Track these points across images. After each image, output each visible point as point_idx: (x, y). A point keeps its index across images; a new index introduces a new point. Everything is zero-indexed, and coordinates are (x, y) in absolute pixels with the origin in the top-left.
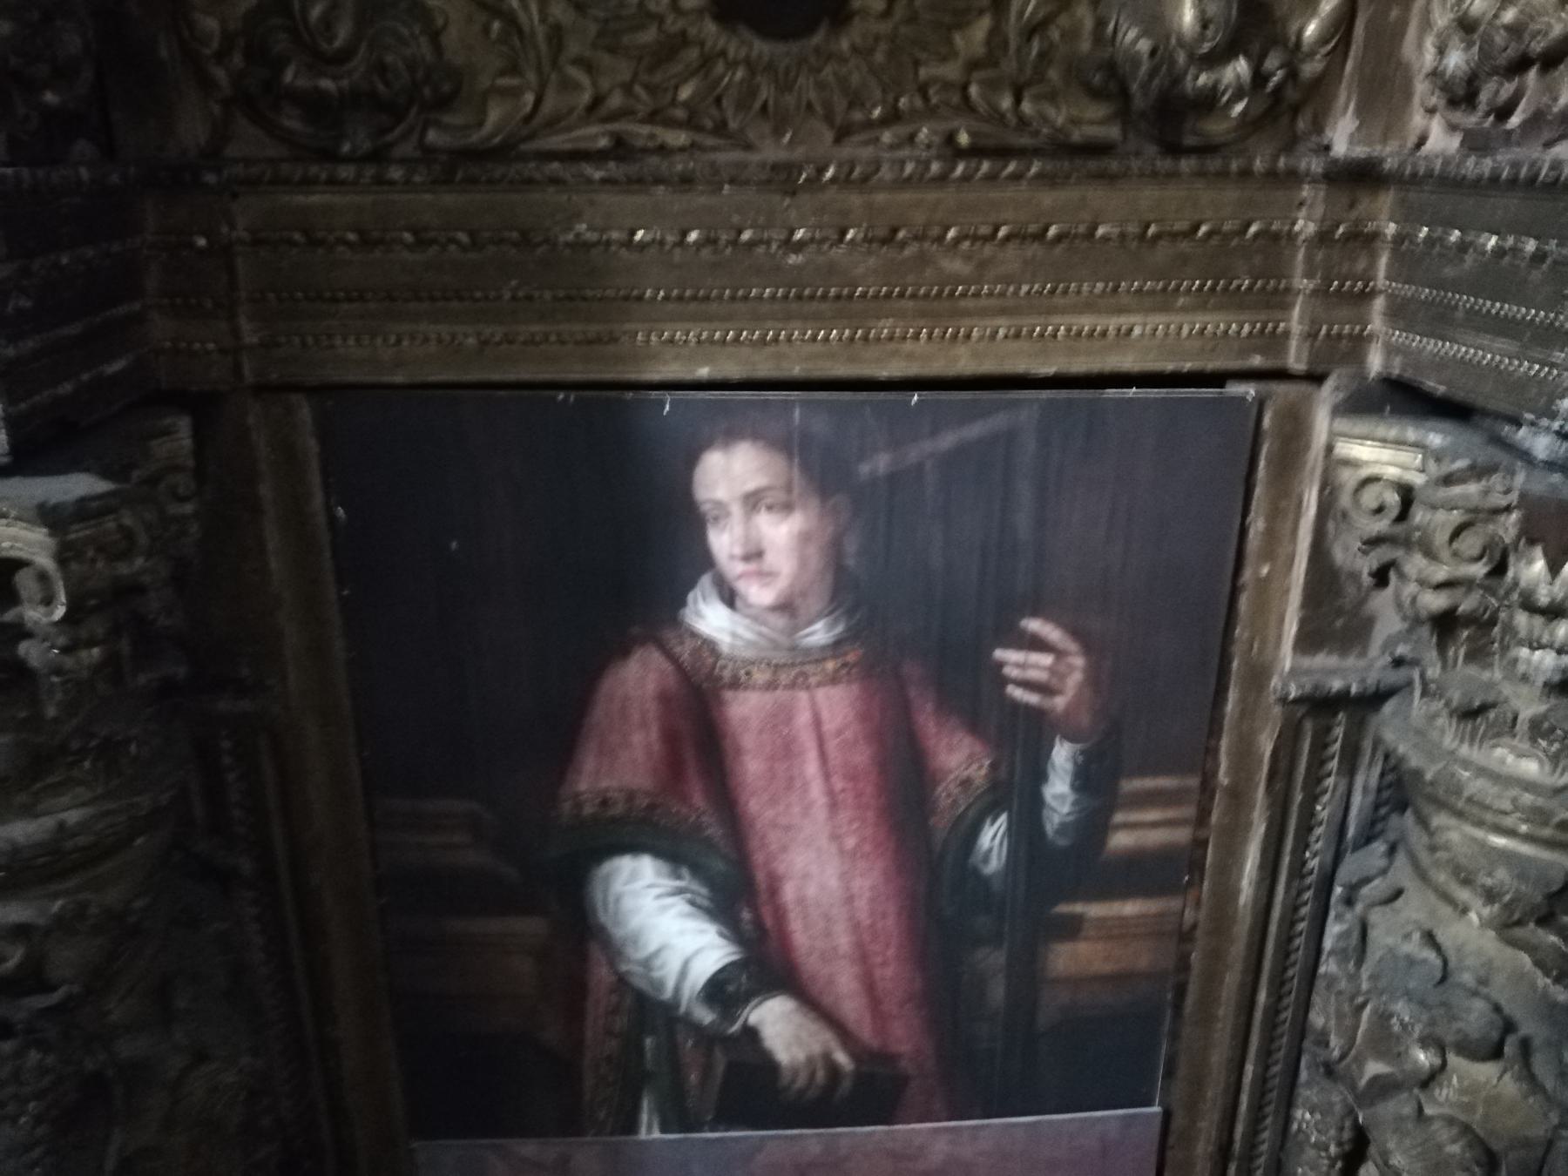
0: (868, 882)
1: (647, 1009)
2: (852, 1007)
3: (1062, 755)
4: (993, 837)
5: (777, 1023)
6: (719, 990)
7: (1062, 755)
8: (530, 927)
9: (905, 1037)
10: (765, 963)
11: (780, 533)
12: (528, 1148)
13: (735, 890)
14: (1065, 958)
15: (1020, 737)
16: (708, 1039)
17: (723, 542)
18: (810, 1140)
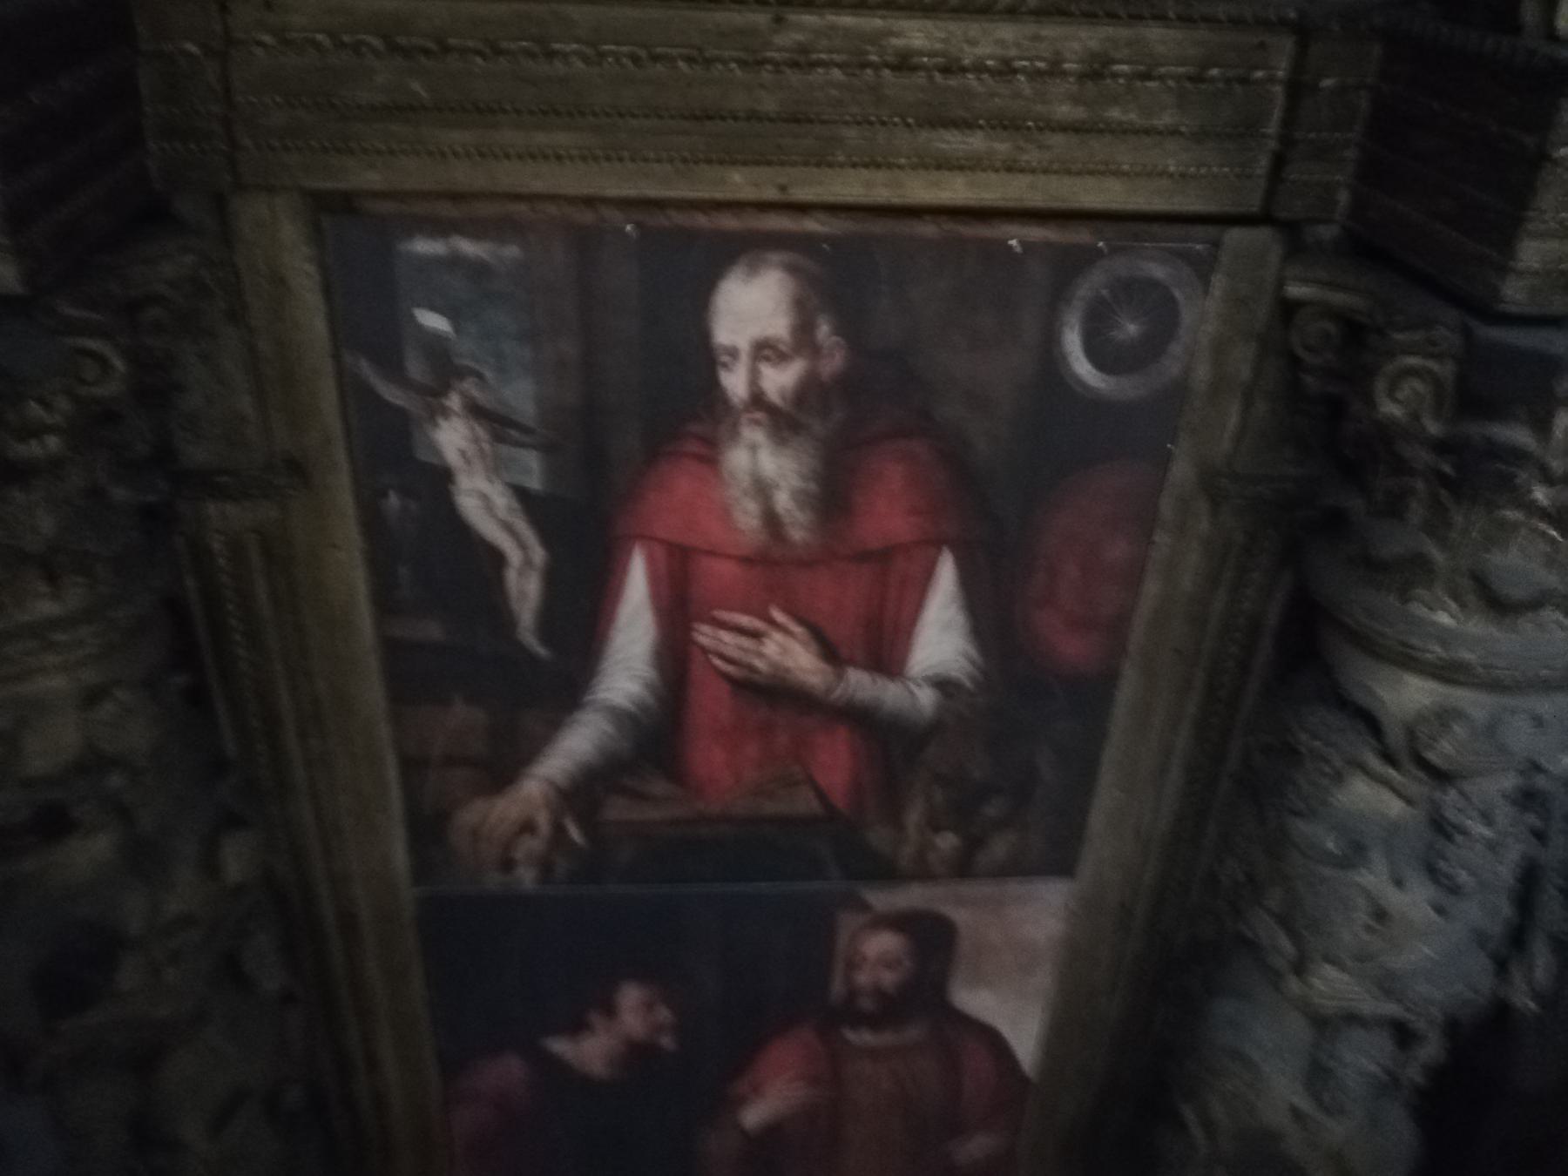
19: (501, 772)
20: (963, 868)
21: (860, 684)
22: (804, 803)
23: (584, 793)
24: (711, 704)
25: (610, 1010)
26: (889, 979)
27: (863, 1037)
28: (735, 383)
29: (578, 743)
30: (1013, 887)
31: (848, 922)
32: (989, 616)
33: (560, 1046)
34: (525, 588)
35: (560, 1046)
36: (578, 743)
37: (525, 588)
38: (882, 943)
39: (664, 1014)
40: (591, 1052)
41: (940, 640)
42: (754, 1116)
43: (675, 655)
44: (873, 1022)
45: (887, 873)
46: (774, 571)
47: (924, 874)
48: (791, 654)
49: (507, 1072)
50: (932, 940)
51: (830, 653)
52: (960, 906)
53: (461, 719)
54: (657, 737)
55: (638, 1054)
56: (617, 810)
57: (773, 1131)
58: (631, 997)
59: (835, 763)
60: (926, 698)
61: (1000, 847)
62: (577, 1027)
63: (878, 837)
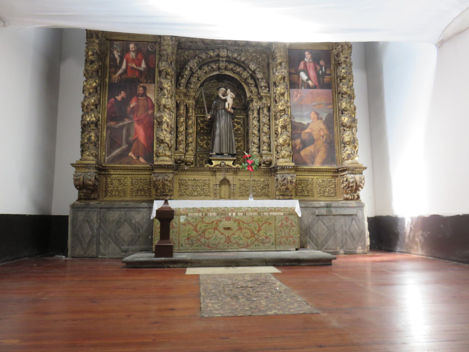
0: (314, 74)
1: (303, 81)
2: (314, 81)
3: (323, 68)
4: (320, 72)
5: (310, 82)
6: (307, 80)
7: (323, 68)
8: (296, 76)
9: (317, 84)
10: (309, 79)
11: (309, 56)
12: (296, 90)
13: (307, 74)
14: (325, 79)
15: (321, 67)
16: (306, 83)
17: (306, 56)
18: (312, 90)
19: (115, 73)
20: (147, 82)
21: (138, 68)
22: (135, 77)
23: (120, 75)
24: (129, 69)
25: (121, 94)
26: (142, 92)
27: (140, 98)
28: (131, 49)
29: (120, 71)
30: (150, 84)
31: (138, 87)
32: (147, 64)
33: (117, 97)
34: (118, 61)
35: (117, 97)
36: (120, 71)
37: (118, 61)
38: (141, 89)
39: (125, 94)
40: (119, 98)
41: (143, 65)
42: (132, 106)
43: (127, 65)
44: (141, 96)
45: (141, 83)
46: (133, 61)
47: (143, 83)
48: (134, 65)
49: (112, 100)
50: (145, 88)
51: (136, 66)
52: (147, 86)
53: (113, 69)
54: (125, 71)
55: (123, 98)
56: (123, 77)
57: (133, 107)
58: (122, 92)
59: (137, 74)
60: (143, 69)
61: (149, 81)
62: (118, 95)
63: (140, 80)
